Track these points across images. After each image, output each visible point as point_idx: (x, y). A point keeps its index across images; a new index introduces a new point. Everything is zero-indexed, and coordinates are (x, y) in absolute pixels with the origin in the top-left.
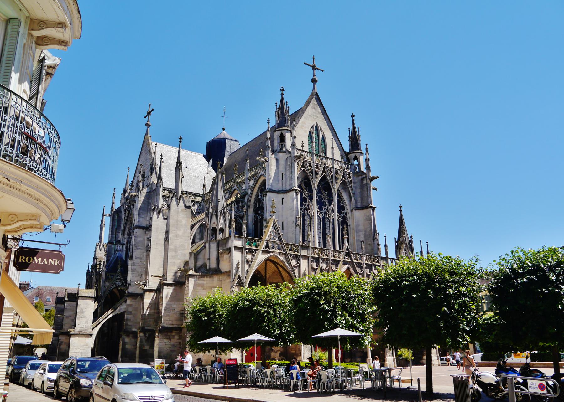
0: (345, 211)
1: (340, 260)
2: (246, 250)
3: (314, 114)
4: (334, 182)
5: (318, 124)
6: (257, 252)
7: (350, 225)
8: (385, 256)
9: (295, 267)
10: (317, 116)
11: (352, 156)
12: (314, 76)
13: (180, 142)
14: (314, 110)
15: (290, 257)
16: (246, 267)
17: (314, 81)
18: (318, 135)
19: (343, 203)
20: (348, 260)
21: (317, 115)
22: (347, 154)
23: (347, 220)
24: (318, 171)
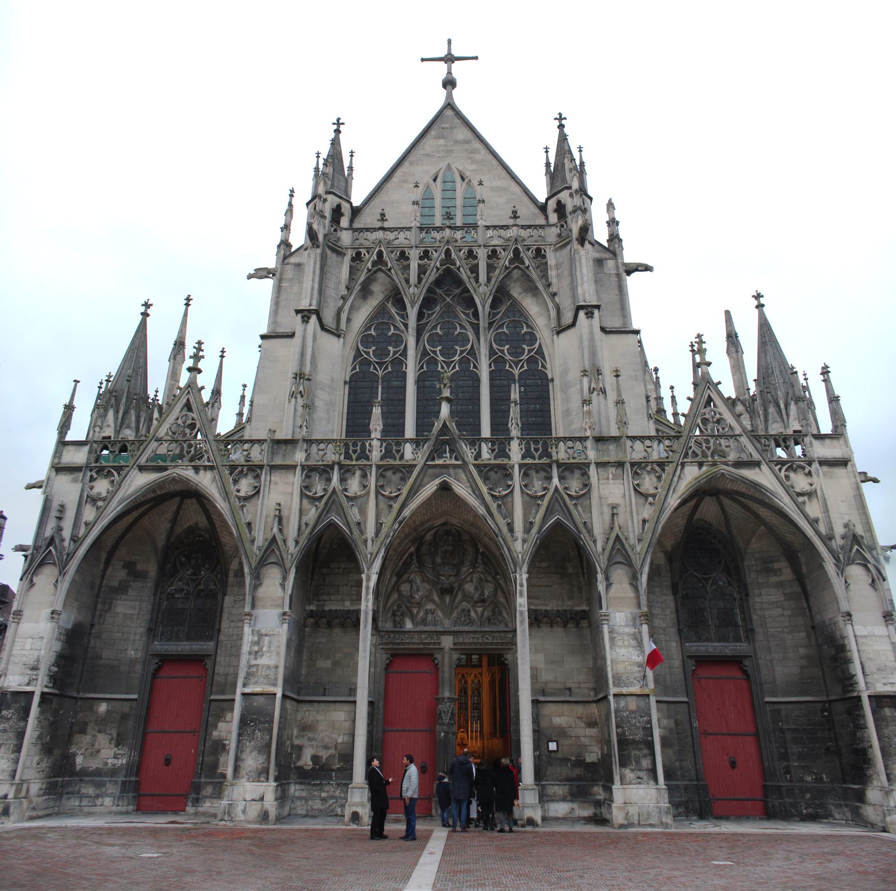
0: (537, 345)
1: (415, 466)
2: (91, 471)
3: (442, 148)
4: (483, 277)
5: (453, 167)
6: (123, 473)
7: (552, 380)
8: (614, 432)
9: (247, 499)
10: (452, 151)
11: (552, 204)
12: (449, 73)
13: (187, 305)
14: (441, 142)
15: (231, 473)
16: (89, 514)
17: (449, 83)
18: (449, 191)
19: (528, 326)
20: (448, 462)
21: (451, 148)
22: (543, 208)
23: (543, 366)
24: (428, 262)
